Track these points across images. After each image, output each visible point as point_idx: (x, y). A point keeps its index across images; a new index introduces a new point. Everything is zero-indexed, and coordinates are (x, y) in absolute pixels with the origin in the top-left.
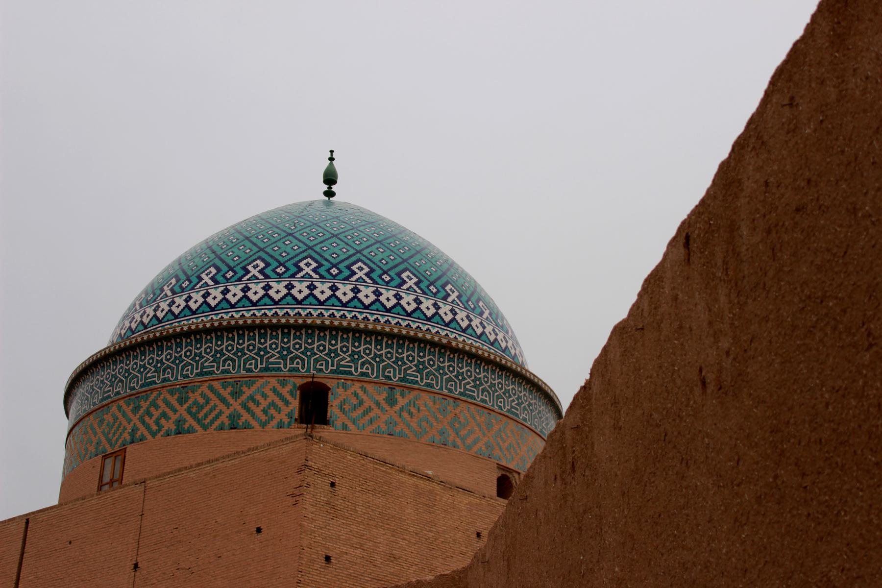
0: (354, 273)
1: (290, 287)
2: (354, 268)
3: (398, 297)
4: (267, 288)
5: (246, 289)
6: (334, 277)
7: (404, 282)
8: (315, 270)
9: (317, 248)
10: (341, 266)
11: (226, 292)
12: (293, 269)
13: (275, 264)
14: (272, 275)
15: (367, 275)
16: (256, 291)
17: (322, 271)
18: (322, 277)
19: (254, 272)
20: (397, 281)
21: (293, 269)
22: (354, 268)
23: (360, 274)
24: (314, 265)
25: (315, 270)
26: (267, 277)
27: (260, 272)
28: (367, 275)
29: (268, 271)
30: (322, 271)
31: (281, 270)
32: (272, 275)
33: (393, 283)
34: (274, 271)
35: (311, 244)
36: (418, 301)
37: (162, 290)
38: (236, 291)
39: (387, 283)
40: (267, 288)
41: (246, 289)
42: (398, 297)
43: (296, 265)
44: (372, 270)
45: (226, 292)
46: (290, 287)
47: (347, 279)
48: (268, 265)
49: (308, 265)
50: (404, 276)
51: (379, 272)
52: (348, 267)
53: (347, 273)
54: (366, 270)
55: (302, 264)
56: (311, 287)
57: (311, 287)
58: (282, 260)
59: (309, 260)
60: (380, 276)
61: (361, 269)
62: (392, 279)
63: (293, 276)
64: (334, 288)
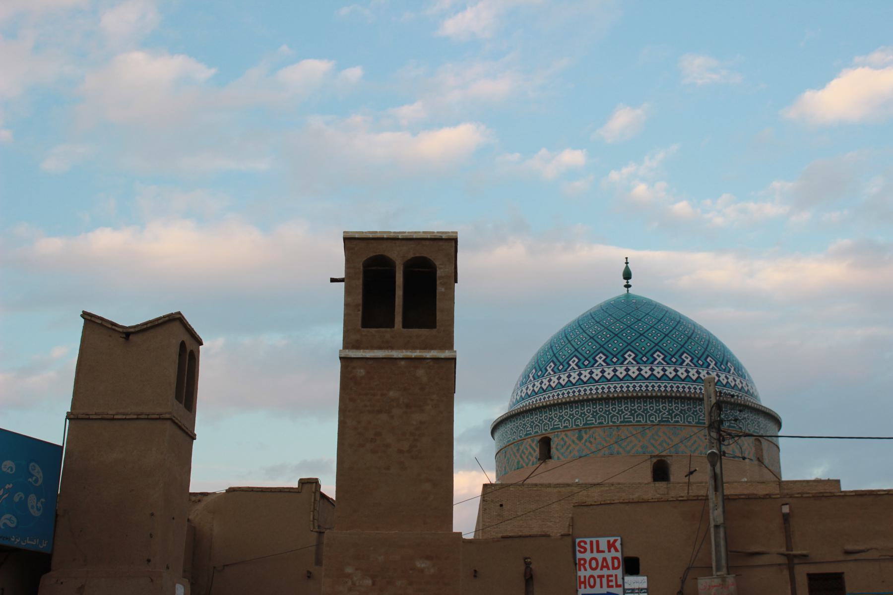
0: (626, 359)
1: (591, 373)
2: (626, 356)
4: (580, 374)
5: (569, 376)
6: (615, 363)
7: (655, 359)
8: (604, 361)
10: (619, 356)
11: (559, 378)
12: (593, 362)
13: (583, 359)
14: (582, 366)
15: (633, 359)
16: (574, 377)
17: (608, 360)
18: (608, 364)
19: (573, 365)
20: (651, 359)
22: (626, 356)
23: (630, 359)
24: (604, 357)
25: (604, 361)
26: (579, 368)
27: (576, 365)
28: (633, 359)
30: (608, 360)
31: (586, 363)
32: (582, 366)
33: (649, 362)
36: (664, 370)
38: (564, 377)
39: (645, 362)
40: (580, 374)
41: (569, 376)
42: (652, 370)
43: (594, 358)
45: (559, 378)
46: (591, 373)
47: (622, 363)
48: (580, 360)
49: (600, 358)
50: (655, 356)
52: (623, 356)
54: (633, 355)
55: (597, 358)
56: (603, 372)
57: (603, 372)
58: (614, 353)
59: (601, 355)
61: (630, 356)
64: (615, 371)
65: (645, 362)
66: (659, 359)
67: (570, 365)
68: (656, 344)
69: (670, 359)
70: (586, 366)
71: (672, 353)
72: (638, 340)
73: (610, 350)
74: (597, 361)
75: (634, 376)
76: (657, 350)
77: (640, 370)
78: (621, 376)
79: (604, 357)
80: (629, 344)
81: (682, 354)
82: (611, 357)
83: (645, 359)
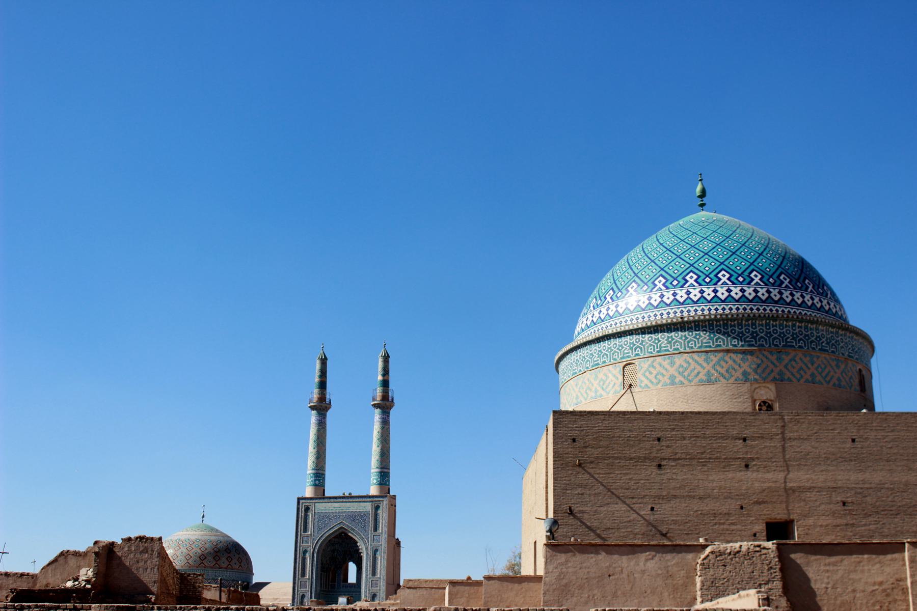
3: (780, 293)
6: (741, 283)
8: (728, 279)
9: (695, 265)
12: (715, 280)
18: (733, 283)
19: (691, 281)
21: (715, 280)
23: (757, 280)
25: (728, 279)
26: (700, 285)
29: (700, 280)
34: (704, 280)
35: (692, 262)
37: (605, 298)
41: (688, 293)
43: (716, 276)
44: (731, 276)
45: (675, 294)
46: (715, 291)
47: (749, 283)
48: (699, 277)
49: (724, 276)
51: (735, 275)
53: (748, 280)
55: (720, 275)
56: (729, 291)
57: (729, 291)
60: (737, 279)
62: (745, 280)
63: (716, 284)
65: (708, 283)
66: (724, 279)
67: (687, 281)
68: (722, 263)
69: (768, 280)
70: (708, 283)
71: (770, 274)
72: (701, 260)
73: (702, 269)
74: (720, 279)
75: (723, 297)
76: (753, 270)
77: (702, 292)
78: (695, 299)
79: (728, 276)
80: (722, 263)
81: (780, 275)
82: (735, 275)
83: (741, 279)
